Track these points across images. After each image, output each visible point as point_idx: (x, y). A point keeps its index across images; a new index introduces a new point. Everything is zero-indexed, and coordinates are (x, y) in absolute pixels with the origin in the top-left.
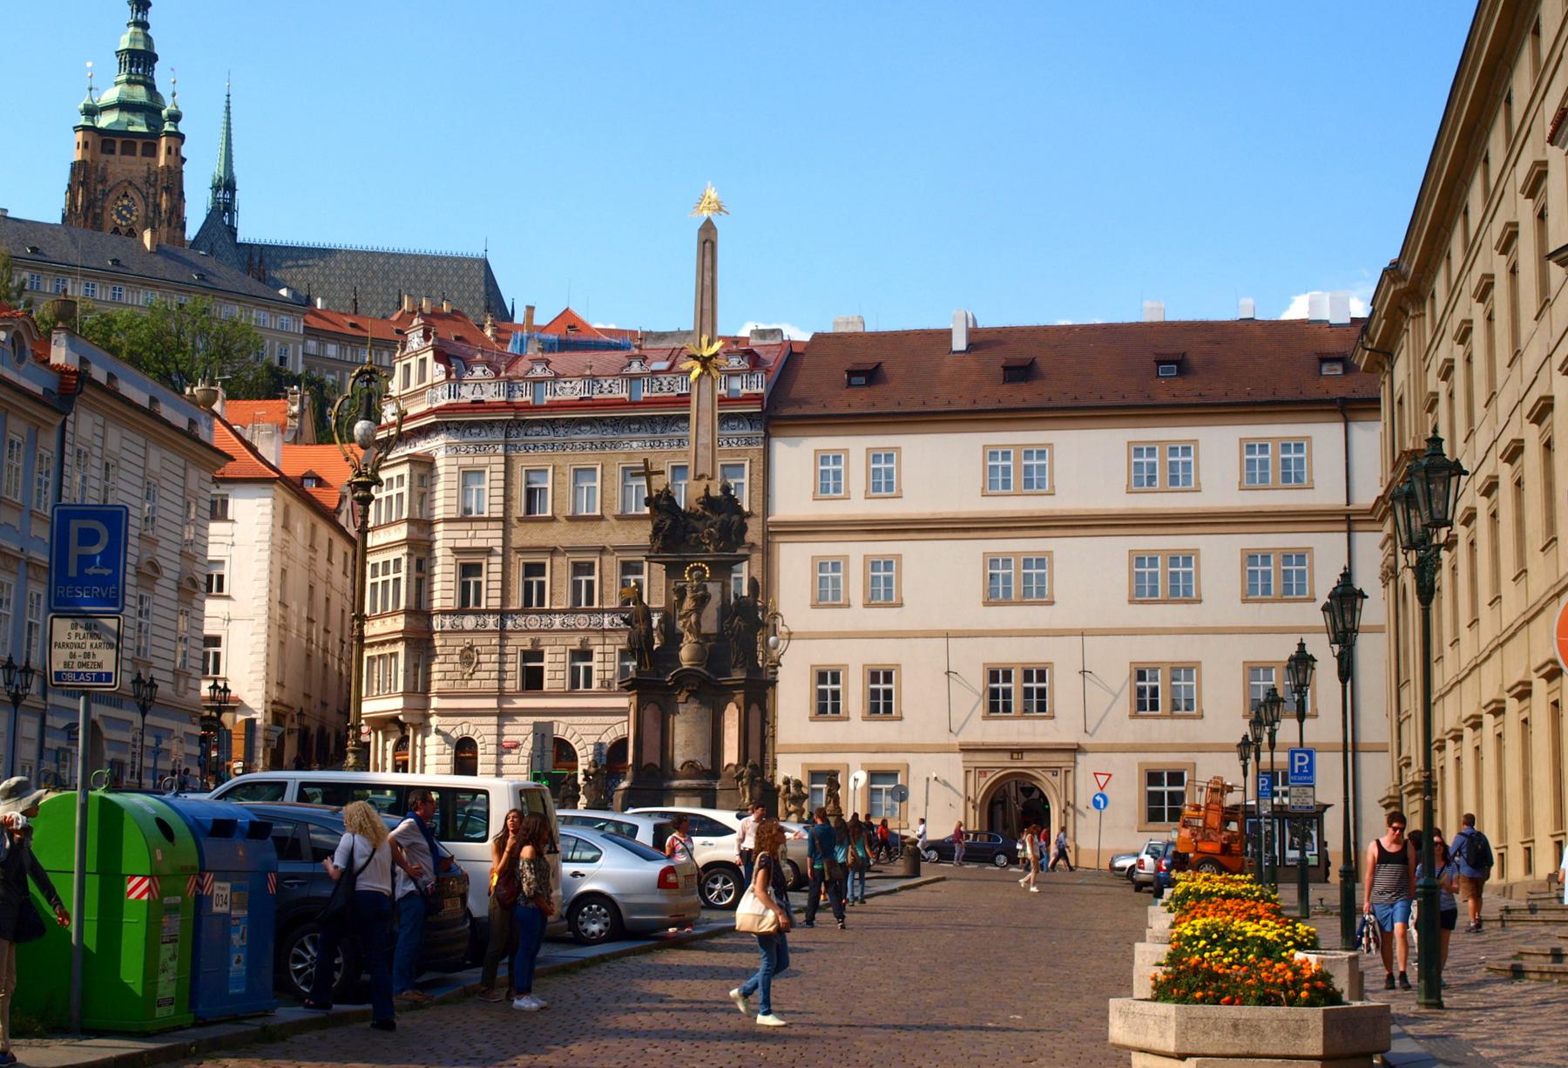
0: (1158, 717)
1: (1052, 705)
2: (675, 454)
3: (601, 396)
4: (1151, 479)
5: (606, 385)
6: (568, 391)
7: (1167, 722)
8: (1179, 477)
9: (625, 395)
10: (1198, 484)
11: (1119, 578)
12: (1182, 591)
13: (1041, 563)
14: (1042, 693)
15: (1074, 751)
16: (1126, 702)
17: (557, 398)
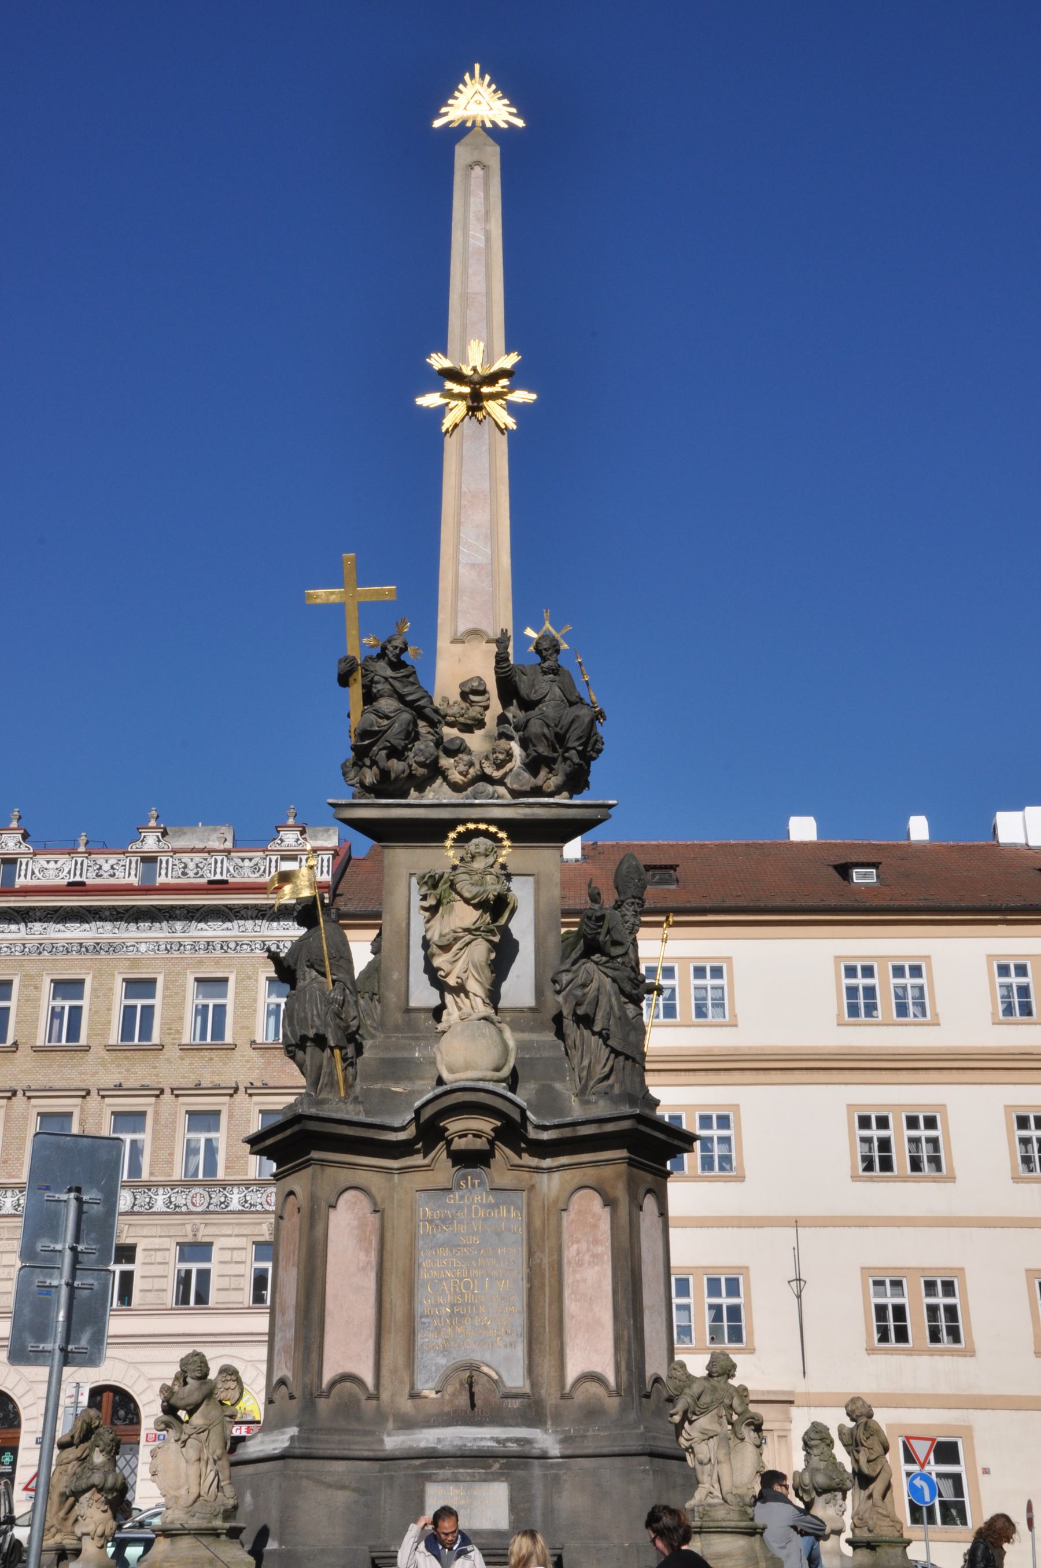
0: (910, 1352)
1: (751, 1334)
2: (201, 962)
3: (99, 881)
4: (871, 1008)
5: (106, 867)
6: (52, 873)
7: (924, 1360)
8: (911, 1006)
9: (134, 880)
10: (936, 1015)
11: (842, 1146)
12: (930, 1160)
13: (724, 1122)
14: (735, 1312)
15: (791, 1402)
16: (860, 1325)
17: (35, 882)
